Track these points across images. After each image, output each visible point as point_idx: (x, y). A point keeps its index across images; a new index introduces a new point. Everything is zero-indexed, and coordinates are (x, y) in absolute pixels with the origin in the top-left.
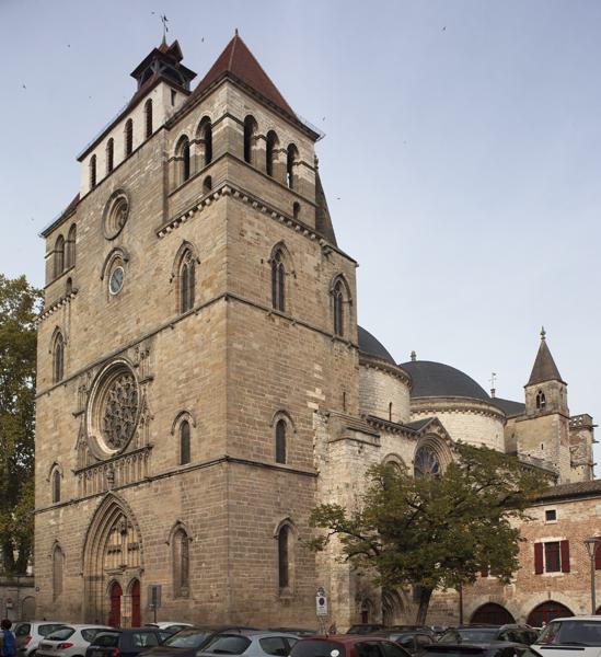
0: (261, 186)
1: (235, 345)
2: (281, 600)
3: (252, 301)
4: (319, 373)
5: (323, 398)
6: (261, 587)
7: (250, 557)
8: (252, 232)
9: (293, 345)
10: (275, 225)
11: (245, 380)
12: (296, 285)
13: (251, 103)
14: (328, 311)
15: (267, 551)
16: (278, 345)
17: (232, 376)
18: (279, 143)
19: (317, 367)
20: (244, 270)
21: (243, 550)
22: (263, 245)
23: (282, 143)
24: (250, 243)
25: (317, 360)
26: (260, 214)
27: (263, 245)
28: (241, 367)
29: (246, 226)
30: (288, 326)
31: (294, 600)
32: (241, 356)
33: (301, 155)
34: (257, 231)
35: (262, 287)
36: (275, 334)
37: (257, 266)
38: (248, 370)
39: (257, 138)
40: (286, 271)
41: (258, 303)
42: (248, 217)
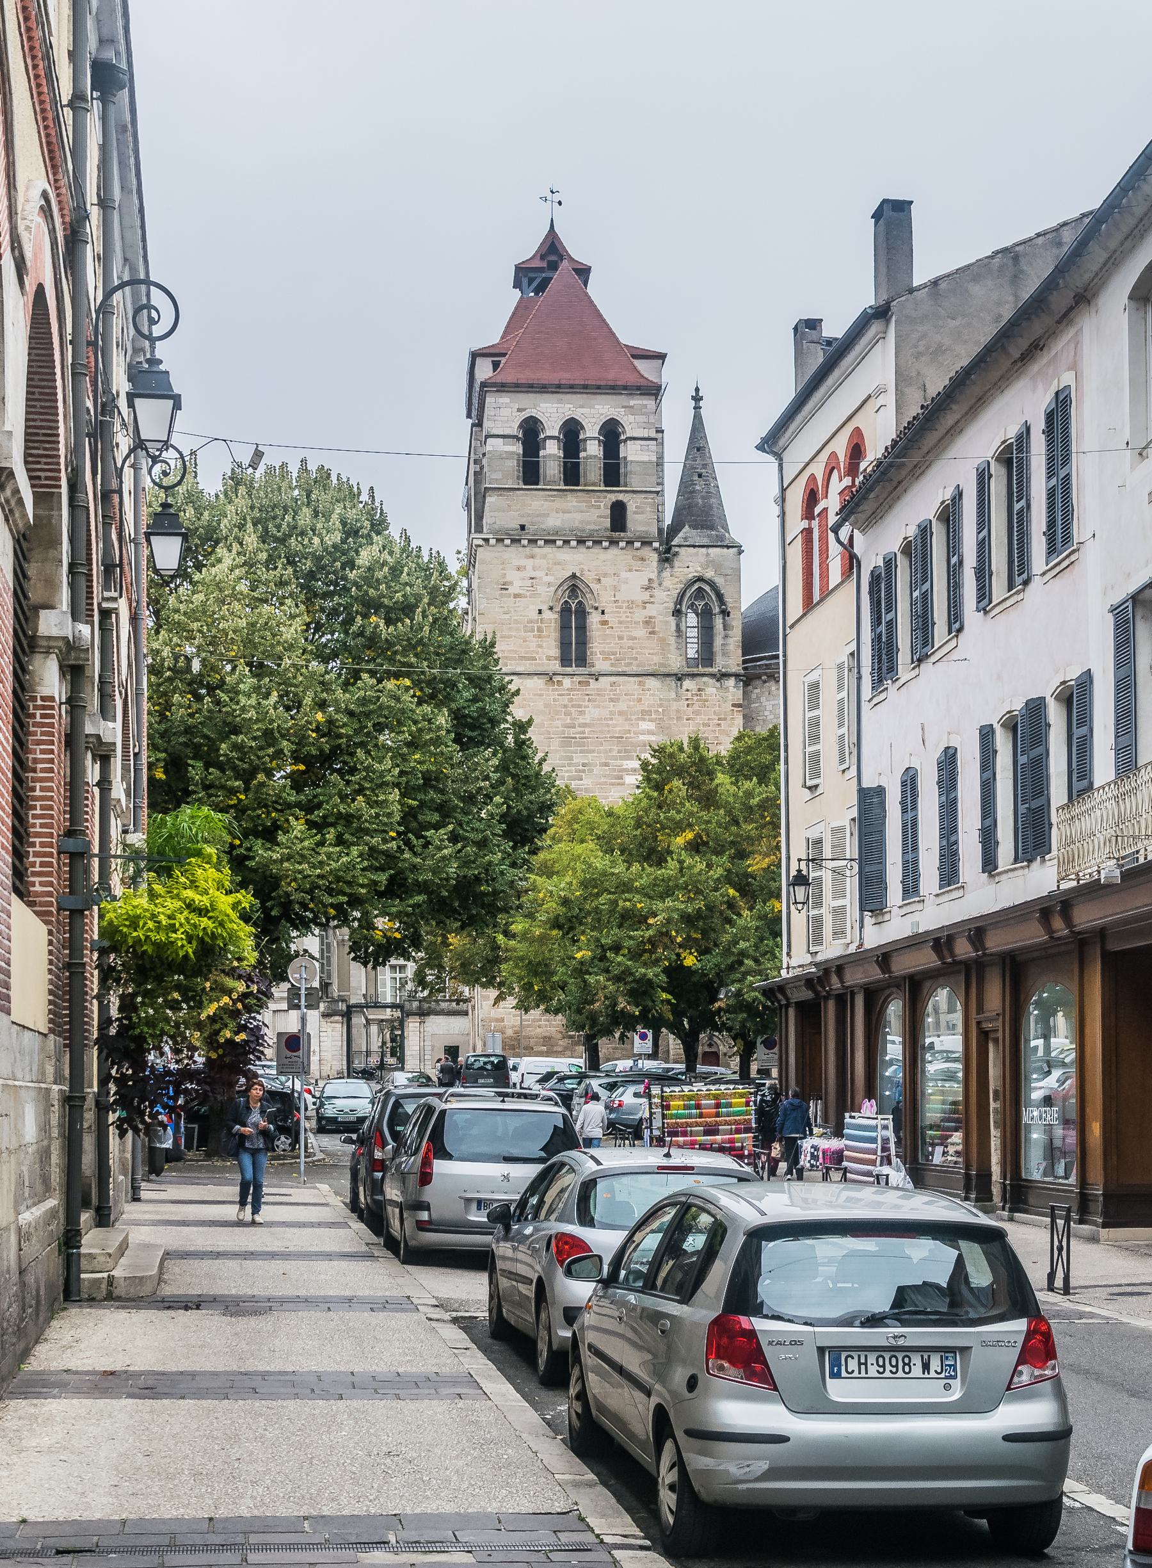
4: (650, 732)
12: (605, 623)
16: (567, 714)
19: (645, 725)
24: (516, 596)
25: (645, 714)
26: (536, 550)
27: (541, 589)
29: (512, 576)
30: (588, 683)
36: (565, 700)
37: (531, 621)
41: (532, 669)
42: (516, 562)
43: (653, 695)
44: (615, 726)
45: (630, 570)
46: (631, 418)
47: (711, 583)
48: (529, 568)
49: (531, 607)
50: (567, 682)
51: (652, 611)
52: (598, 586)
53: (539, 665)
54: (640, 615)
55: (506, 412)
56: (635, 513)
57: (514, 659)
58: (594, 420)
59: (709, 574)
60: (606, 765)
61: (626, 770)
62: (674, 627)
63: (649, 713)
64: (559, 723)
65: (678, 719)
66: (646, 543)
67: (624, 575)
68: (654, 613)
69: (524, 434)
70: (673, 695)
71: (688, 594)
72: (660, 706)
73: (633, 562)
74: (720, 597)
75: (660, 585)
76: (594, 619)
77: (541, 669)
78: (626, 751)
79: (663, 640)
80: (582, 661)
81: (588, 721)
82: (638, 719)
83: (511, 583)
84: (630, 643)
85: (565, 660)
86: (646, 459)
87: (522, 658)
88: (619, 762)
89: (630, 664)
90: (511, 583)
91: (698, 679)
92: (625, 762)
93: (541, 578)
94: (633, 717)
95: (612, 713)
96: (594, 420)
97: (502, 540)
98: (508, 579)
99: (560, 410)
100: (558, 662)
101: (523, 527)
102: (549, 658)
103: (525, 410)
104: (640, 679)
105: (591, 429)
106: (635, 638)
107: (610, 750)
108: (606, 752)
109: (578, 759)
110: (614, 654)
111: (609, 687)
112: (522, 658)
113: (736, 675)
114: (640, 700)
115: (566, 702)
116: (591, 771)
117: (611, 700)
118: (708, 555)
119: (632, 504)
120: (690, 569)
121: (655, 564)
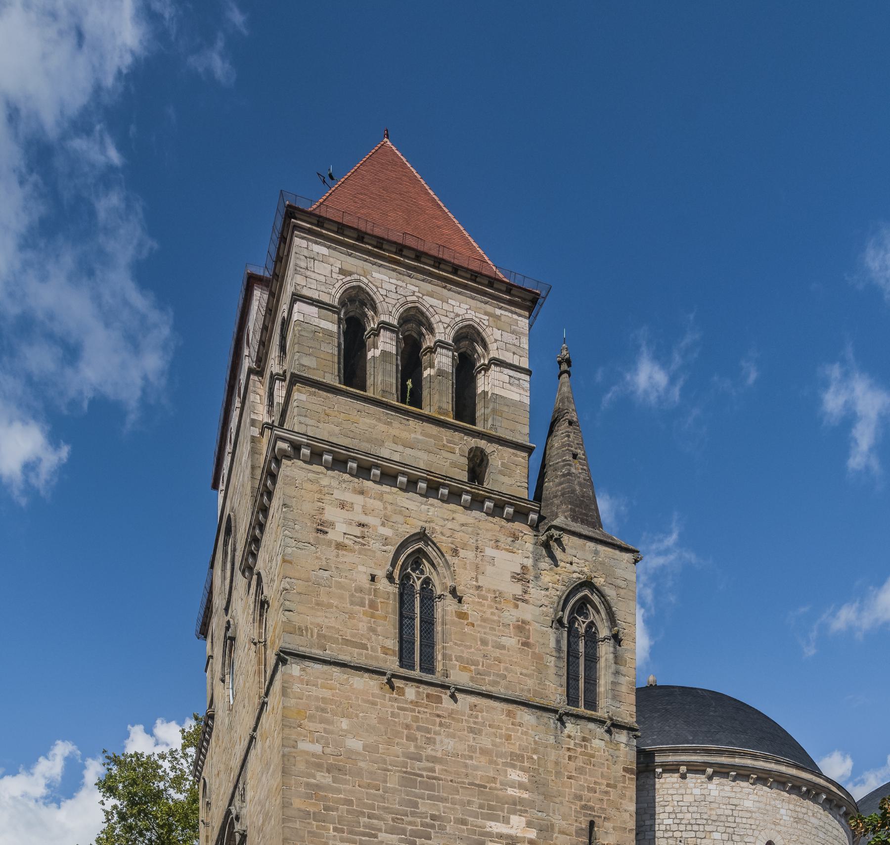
1: (303, 746)
3: (344, 657)
4: (521, 786)
5: (532, 834)
8: (349, 523)
9: (453, 736)
10: (411, 502)
11: (327, 808)
12: (462, 616)
13: (353, 263)
14: (551, 661)
17: (297, 803)
18: (431, 330)
19: (515, 775)
20: (324, 598)
22: (376, 545)
23: (439, 329)
24: (340, 546)
25: (515, 759)
26: (369, 484)
27: (376, 545)
28: (318, 787)
29: (331, 513)
32: (319, 766)
33: (492, 347)
35: (372, 630)
36: (407, 717)
37: (360, 590)
38: (339, 791)
39: (376, 333)
40: (438, 591)
42: (338, 495)
43: (526, 733)
44: (476, 768)
45: (497, 547)
46: (497, 334)
47: (602, 595)
48: (358, 508)
49: (361, 568)
50: (411, 692)
51: (527, 612)
54: (511, 615)
55: (322, 269)
57: (335, 641)
58: (447, 320)
59: (599, 581)
60: (464, 822)
61: (489, 835)
62: (553, 644)
63: (520, 758)
64: (398, 750)
65: (558, 774)
66: (520, 514)
67: (489, 552)
68: (528, 617)
70: (552, 740)
71: (572, 602)
72: (535, 751)
73: (502, 538)
75: (537, 578)
76: (445, 609)
77: (373, 664)
78: (490, 808)
79: (538, 658)
80: (428, 665)
81: (439, 754)
82: (506, 764)
83: (332, 525)
84: (497, 653)
85: (405, 655)
86: (516, 397)
87: (346, 642)
88: (480, 821)
89: (495, 683)
90: (332, 525)
91: (583, 723)
92: (489, 823)
94: (500, 761)
95: (472, 749)
96: (447, 320)
99: (400, 291)
100: (396, 659)
102: (385, 651)
104: (511, 707)
105: (443, 332)
106: (503, 647)
107: (469, 803)
108: (462, 804)
109: (424, 807)
110: (476, 663)
111: (468, 711)
113: (631, 729)
114: (508, 738)
115: (409, 720)
116: (442, 828)
117: (471, 730)
118: (596, 553)
120: (574, 567)
121: (530, 546)
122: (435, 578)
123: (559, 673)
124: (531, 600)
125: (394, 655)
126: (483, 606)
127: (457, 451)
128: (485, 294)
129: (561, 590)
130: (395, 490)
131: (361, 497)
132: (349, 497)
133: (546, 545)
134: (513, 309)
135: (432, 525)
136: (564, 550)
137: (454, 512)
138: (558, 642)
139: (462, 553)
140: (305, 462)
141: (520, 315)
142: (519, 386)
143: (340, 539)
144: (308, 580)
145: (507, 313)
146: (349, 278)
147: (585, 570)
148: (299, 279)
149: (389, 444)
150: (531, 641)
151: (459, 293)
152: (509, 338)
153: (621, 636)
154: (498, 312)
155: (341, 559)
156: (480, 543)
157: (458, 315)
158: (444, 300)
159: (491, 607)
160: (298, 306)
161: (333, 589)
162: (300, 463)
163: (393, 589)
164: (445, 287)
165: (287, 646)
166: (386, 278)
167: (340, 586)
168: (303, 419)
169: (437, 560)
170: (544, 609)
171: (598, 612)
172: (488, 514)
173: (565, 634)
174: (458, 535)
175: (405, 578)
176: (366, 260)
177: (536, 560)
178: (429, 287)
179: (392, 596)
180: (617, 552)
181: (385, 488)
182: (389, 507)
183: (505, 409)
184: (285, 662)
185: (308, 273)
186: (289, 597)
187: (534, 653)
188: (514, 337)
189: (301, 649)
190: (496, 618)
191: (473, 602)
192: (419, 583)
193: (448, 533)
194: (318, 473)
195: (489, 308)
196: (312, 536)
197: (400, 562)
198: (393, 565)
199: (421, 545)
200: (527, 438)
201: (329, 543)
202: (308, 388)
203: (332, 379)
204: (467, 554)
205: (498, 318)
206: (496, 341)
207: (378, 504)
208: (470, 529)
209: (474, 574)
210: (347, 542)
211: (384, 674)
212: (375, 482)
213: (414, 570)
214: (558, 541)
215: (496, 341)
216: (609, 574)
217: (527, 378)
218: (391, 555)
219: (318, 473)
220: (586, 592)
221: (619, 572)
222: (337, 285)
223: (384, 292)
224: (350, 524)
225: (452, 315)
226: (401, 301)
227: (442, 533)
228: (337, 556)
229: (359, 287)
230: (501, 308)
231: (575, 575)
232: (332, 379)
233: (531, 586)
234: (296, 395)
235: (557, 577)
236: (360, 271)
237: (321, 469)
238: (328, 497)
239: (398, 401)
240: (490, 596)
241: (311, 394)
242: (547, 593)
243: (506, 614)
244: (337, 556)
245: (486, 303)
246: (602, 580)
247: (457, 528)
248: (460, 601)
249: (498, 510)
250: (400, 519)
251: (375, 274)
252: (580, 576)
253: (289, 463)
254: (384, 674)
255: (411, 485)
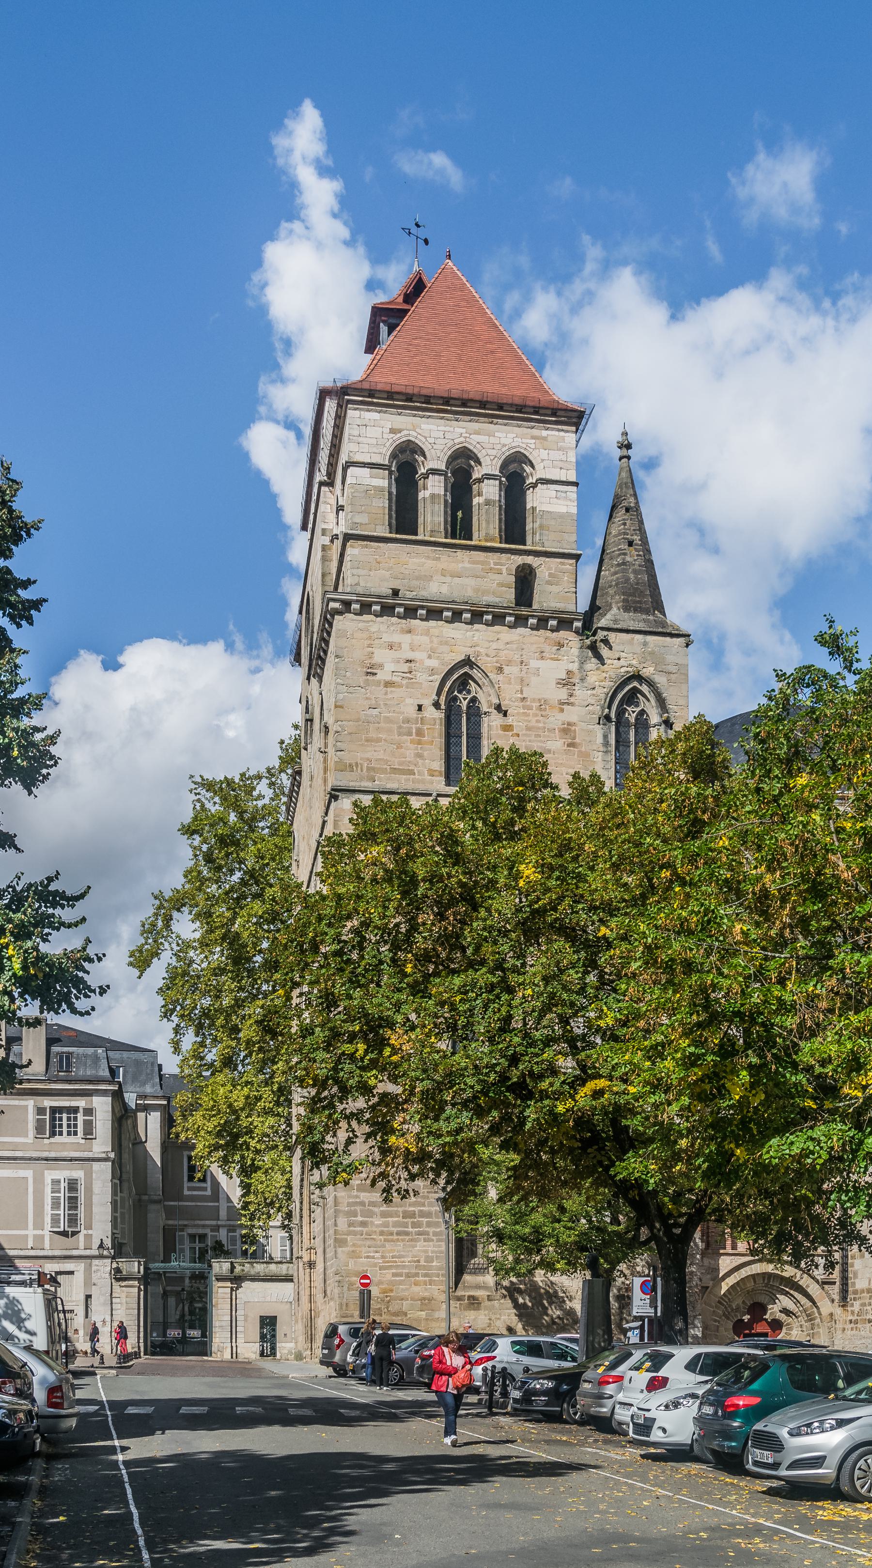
0: (430, 563)
2: (459, 1299)
6: (408, 1275)
7: (386, 1225)
15: (422, 1214)
20: (373, 735)
21: (371, 1214)
24: (388, 684)
26: (416, 622)
27: (422, 677)
29: (381, 655)
31: (489, 1298)
34: (410, 655)
35: (419, 756)
37: (407, 721)
40: (484, 708)
42: (386, 638)
45: (542, 658)
46: (544, 454)
47: (651, 684)
48: (406, 646)
49: (409, 701)
51: (572, 714)
52: (500, 677)
53: (419, 781)
54: (556, 720)
56: (549, 583)
57: (384, 771)
59: (648, 671)
62: (600, 739)
66: (564, 623)
67: (534, 663)
68: (573, 718)
69: (400, 468)
71: (620, 696)
74: (662, 703)
75: (582, 680)
83: (381, 666)
86: (563, 510)
87: (394, 771)
90: (381, 666)
93: (422, 662)
96: (494, 452)
97: (370, 605)
98: (377, 659)
99: (448, 436)
100: (442, 779)
101: (396, 593)
102: (432, 773)
103: (400, 431)
105: (489, 464)
112: (394, 771)
118: (645, 644)
119: (544, 568)
121: (575, 651)
122: (481, 696)
123: (608, 766)
124: (577, 702)
125: (441, 775)
126: (528, 715)
127: (504, 571)
128: (531, 420)
129: (610, 685)
130: (440, 623)
131: (408, 637)
132: (396, 638)
133: (593, 648)
134: (560, 427)
135: (477, 649)
136: (611, 648)
137: (498, 633)
138: (605, 737)
139: (506, 669)
140: (356, 614)
141: (567, 431)
142: (566, 498)
143: (388, 678)
144: (358, 720)
145: (554, 433)
146: (399, 435)
147: (634, 662)
148: (353, 447)
149: (438, 578)
150: (577, 740)
151: (505, 425)
152: (556, 455)
153: (672, 720)
154: (545, 433)
155: (390, 696)
156: (525, 658)
157: (504, 445)
158: (491, 435)
159: (536, 715)
160: (351, 471)
161: (382, 725)
162: (351, 616)
163: (440, 715)
164: (491, 423)
165: (339, 783)
166: (434, 427)
167: (388, 720)
168: (355, 571)
169: (482, 680)
170: (590, 708)
171: (648, 700)
172: (532, 629)
173: (613, 728)
174: (502, 654)
175: (452, 701)
176: (415, 416)
177: (582, 663)
178: (475, 426)
179: (438, 721)
180: (668, 639)
181: (432, 623)
182: (435, 640)
183: (553, 522)
184: (336, 798)
185: (360, 439)
186: (340, 738)
187: (580, 752)
188: (561, 453)
189: (351, 784)
190: (541, 725)
191: (518, 714)
192: (464, 705)
193: (493, 653)
194: (368, 622)
195: (535, 432)
196: (362, 679)
197: (446, 689)
198: (439, 694)
199: (466, 669)
200: (574, 546)
201: (379, 682)
202: (360, 542)
203: (382, 531)
204: (512, 671)
205: (545, 439)
206: (543, 460)
207: (425, 639)
208: (515, 646)
209: (518, 687)
210: (395, 679)
211: (430, 795)
212: (421, 620)
213: (460, 692)
214: (606, 642)
215: (543, 460)
216: (657, 659)
217: (574, 489)
218: (437, 684)
219: (368, 622)
220: (635, 684)
221: (670, 658)
222: (388, 444)
223: (432, 440)
224: (398, 662)
225: (499, 446)
226: (449, 445)
227: (487, 655)
228: (386, 694)
229: (409, 441)
230: (547, 429)
231: (623, 670)
232: (382, 531)
233: (576, 688)
234: (349, 551)
235: (604, 675)
236: (410, 427)
237: (372, 617)
238: (377, 641)
239: (446, 537)
240: (535, 705)
241: (363, 546)
242: (594, 692)
243: (552, 719)
244: (386, 694)
245: (533, 428)
246: (651, 669)
247: (501, 647)
248: (505, 714)
249: (542, 623)
250: (445, 648)
251: (423, 426)
252: (629, 669)
253: (341, 618)
254: (430, 795)
255: (457, 616)
